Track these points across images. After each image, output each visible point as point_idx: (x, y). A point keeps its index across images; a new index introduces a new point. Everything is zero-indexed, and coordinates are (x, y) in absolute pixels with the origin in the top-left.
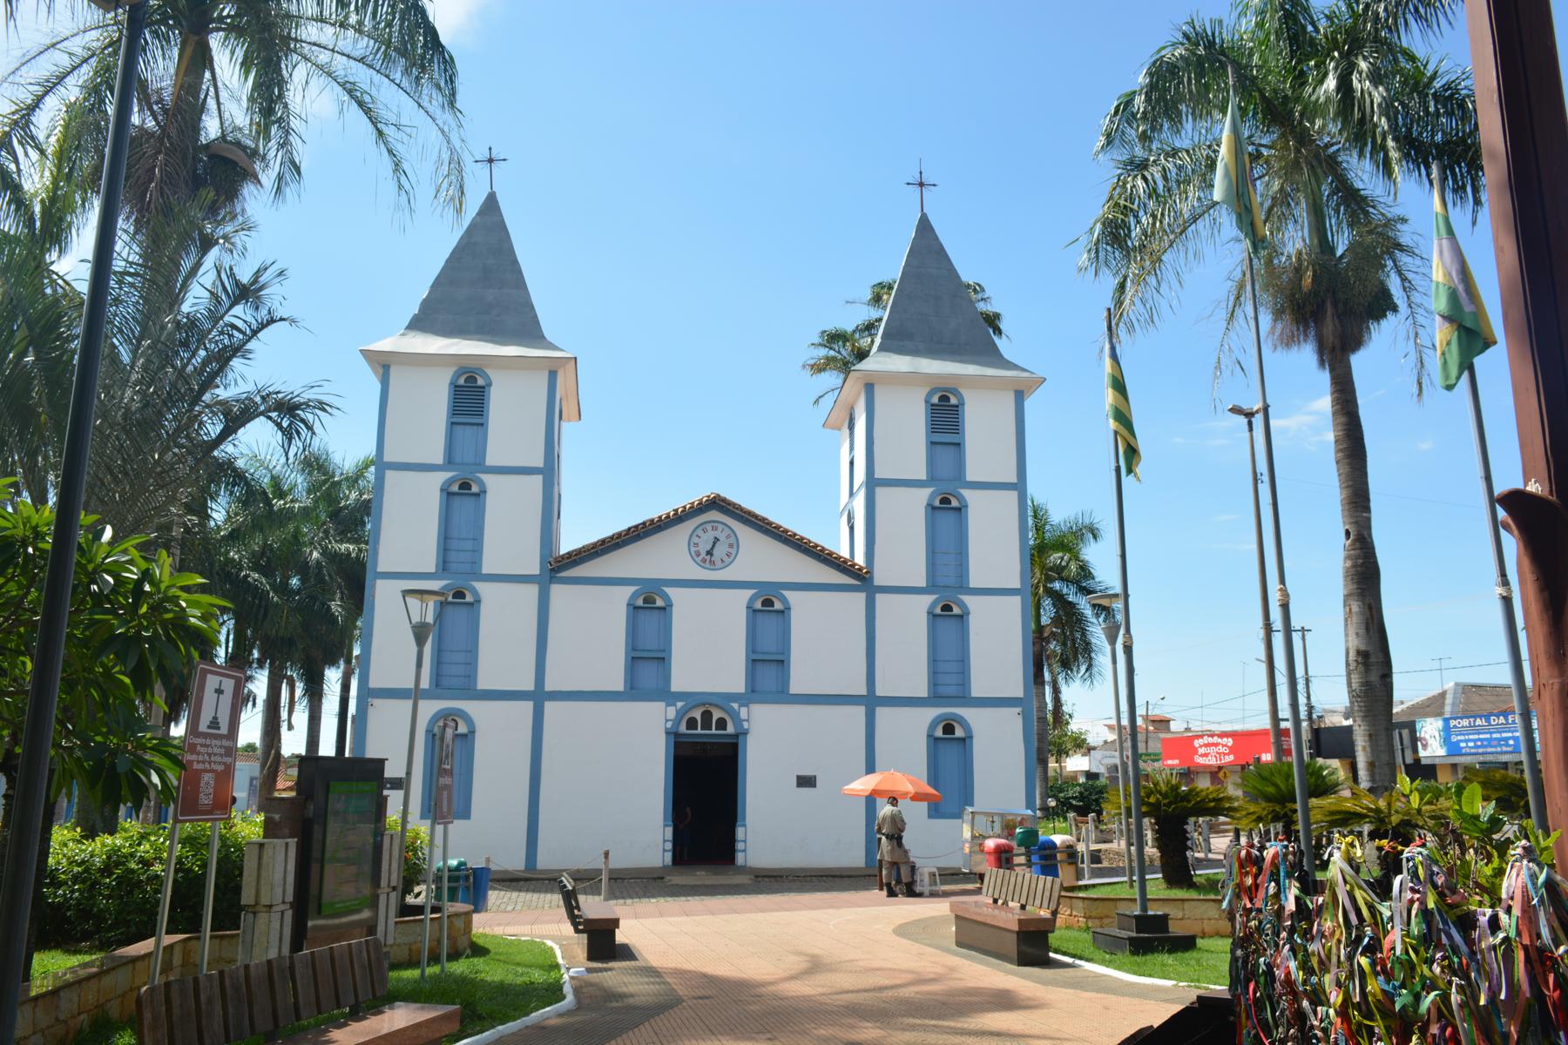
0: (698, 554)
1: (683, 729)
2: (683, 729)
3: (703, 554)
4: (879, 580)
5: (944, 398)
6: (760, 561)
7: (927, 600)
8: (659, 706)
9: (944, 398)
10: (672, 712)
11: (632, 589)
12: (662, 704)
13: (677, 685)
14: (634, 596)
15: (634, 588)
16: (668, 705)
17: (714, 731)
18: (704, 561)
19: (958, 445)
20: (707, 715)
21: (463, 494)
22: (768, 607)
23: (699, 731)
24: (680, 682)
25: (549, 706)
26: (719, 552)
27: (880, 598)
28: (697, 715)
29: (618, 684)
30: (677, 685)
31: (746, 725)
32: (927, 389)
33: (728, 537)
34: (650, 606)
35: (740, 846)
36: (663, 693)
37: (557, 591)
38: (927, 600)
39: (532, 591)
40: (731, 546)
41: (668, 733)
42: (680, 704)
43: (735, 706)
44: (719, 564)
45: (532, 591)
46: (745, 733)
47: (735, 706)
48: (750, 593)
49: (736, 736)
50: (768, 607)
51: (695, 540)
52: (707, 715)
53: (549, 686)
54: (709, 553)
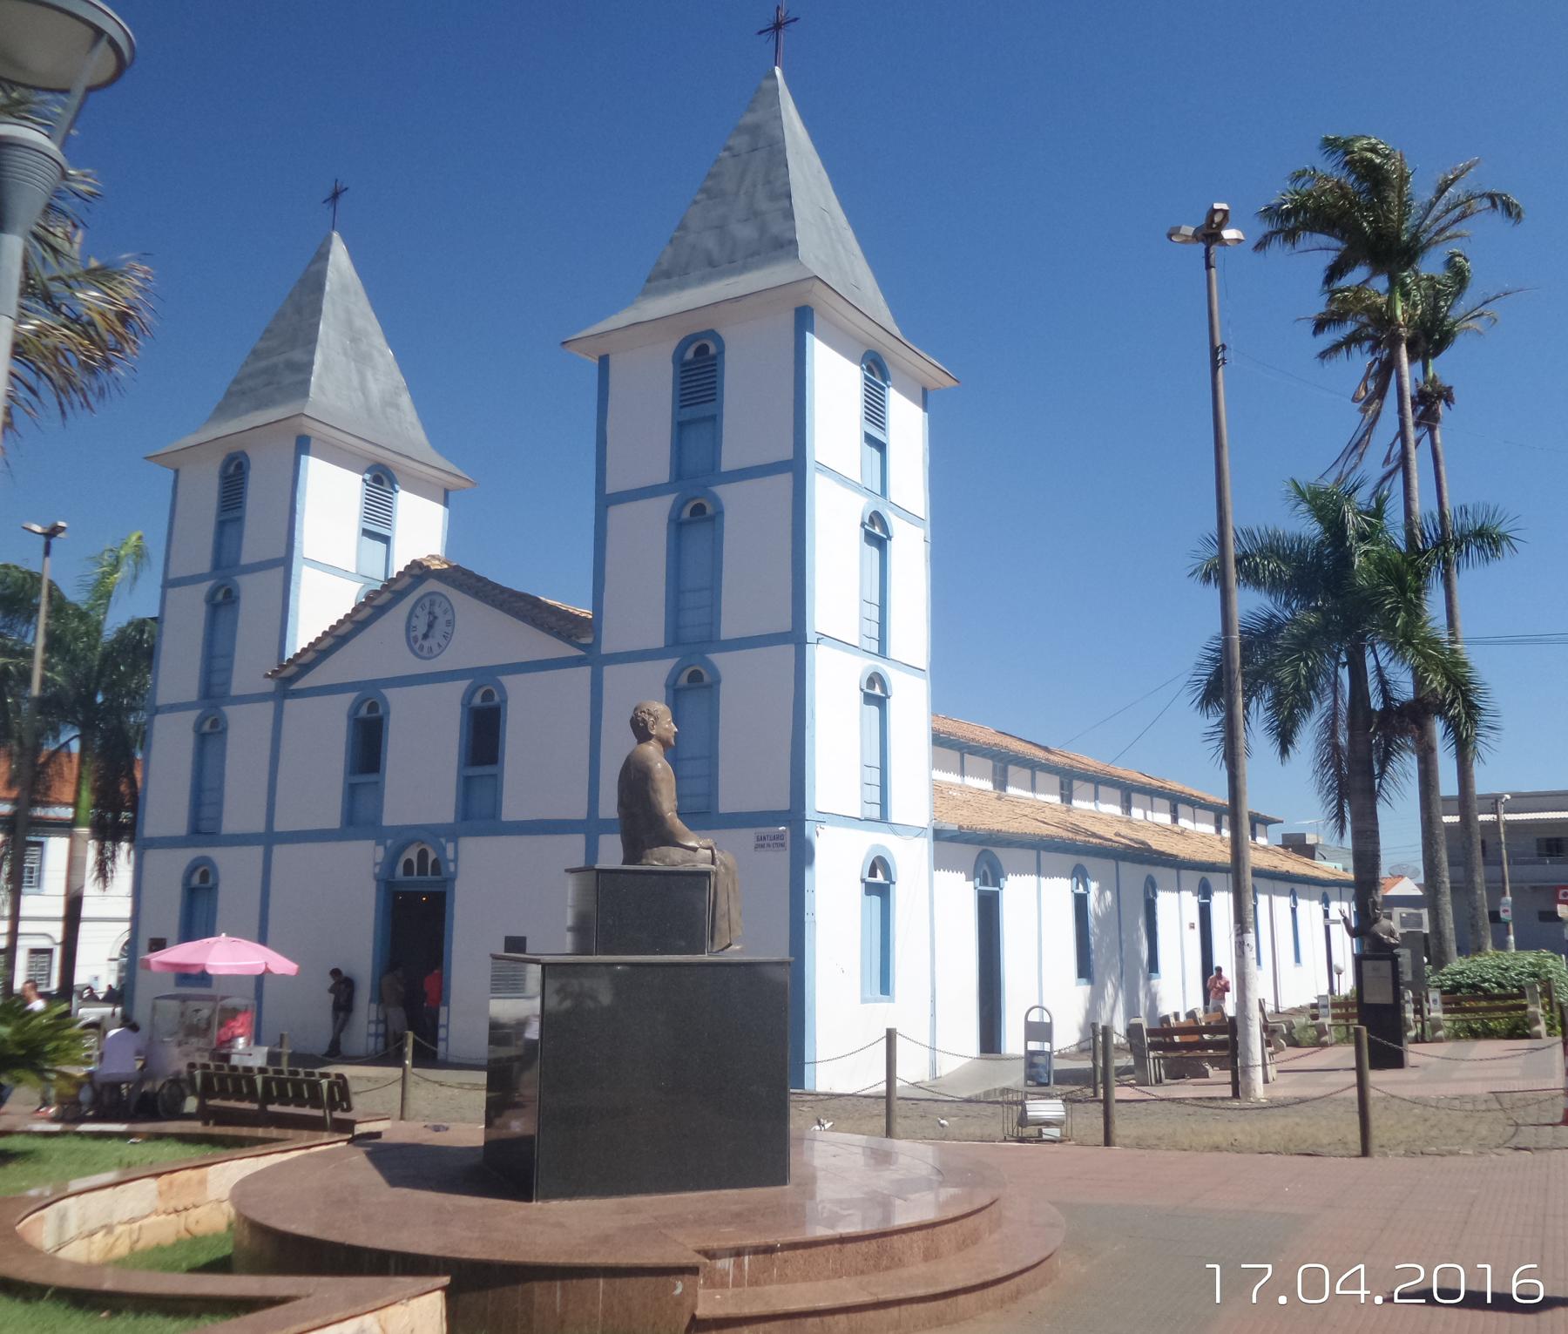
5: (702, 350)
7: (665, 666)
9: (702, 350)
10: (380, 853)
12: (371, 843)
13: (388, 820)
14: (355, 708)
16: (378, 844)
17: (430, 877)
19: (714, 420)
20: (423, 855)
25: (279, 851)
26: (440, 626)
27: (609, 671)
28: (412, 854)
29: (332, 818)
30: (388, 820)
31: (452, 867)
32: (675, 343)
33: (445, 612)
35: (442, 1033)
37: (290, 705)
38: (665, 666)
39: (268, 708)
41: (378, 879)
42: (389, 842)
43: (443, 840)
44: (436, 650)
45: (268, 708)
46: (452, 879)
47: (443, 840)
48: (462, 685)
49: (445, 881)
51: (415, 622)
52: (423, 855)
53: (280, 826)
54: (425, 636)
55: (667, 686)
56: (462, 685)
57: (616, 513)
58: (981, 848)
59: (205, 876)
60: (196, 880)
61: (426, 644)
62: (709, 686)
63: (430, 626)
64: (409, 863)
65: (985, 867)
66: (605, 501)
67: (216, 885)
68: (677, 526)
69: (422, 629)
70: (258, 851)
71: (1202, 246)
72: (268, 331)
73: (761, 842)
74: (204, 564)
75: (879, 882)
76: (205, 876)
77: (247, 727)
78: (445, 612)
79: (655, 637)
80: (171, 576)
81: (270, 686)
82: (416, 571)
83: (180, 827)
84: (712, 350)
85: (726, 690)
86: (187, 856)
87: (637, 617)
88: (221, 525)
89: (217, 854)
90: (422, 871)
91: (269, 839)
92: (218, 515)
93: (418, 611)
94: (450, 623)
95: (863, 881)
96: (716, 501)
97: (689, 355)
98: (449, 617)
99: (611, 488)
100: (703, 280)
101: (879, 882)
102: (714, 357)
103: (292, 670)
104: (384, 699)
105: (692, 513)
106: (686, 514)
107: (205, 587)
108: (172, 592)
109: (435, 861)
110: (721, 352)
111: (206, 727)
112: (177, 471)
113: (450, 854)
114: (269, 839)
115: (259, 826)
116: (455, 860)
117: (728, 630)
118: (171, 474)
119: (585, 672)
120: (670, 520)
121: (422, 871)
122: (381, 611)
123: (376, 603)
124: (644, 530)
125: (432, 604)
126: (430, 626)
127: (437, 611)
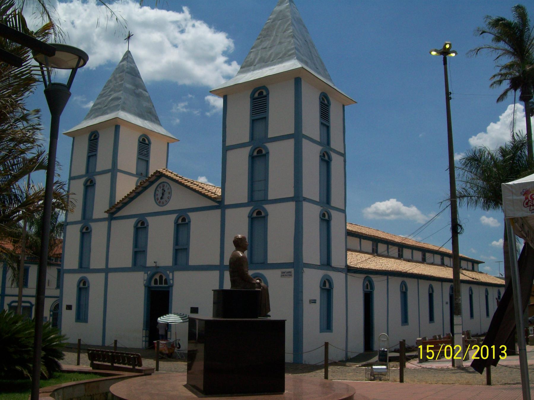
0: (158, 199)
1: (153, 284)
2: (153, 284)
3: (159, 199)
4: (227, 202)
5: (261, 93)
6: (178, 201)
8: (142, 274)
9: (261, 93)
11: (136, 219)
12: (142, 273)
15: (136, 219)
17: (163, 285)
18: (160, 202)
20: (161, 277)
21: (90, 185)
22: (182, 223)
23: (158, 285)
24: (150, 263)
25: (111, 275)
26: (166, 195)
28: (157, 277)
31: (171, 282)
32: (251, 91)
33: (168, 189)
34: (141, 227)
36: (144, 268)
37: (113, 222)
39: (106, 223)
40: (169, 193)
41: (145, 286)
42: (149, 272)
43: (168, 272)
44: (165, 203)
45: (106, 223)
46: (172, 286)
47: (168, 272)
49: (169, 287)
50: (182, 223)
51: (157, 192)
52: (161, 277)
53: (110, 266)
54: (162, 198)
55: (248, 217)
56: (174, 216)
57: (230, 154)
58: (366, 275)
59: (84, 284)
60: (81, 285)
61: (162, 201)
62: (264, 217)
63: (163, 194)
64: (156, 280)
65: (367, 282)
66: (226, 149)
67: (89, 286)
68: (252, 158)
69: (160, 196)
70: (103, 275)
71: (442, 56)
72: (105, 87)
73: (283, 275)
74: (83, 171)
75: (327, 288)
76: (84, 284)
77: (99, 231)
78: (168, 189)
79: (244, 199)
80: (72, 175)
81: (106, 215)
82: (158, 174)
83: (76, 266)
84: (265, 93)
85: (270, 219)
86: (77, 277)
87: (239, 192)
88: (89, 157)
89: (90, 277)
90: (161, 283)
91: (107, 271)
92: (88, 153)
93: (159, 189)
94: (170, 193)
95: (321, 288)
96: (266, 148)
97: (256, 95)
98: (169, 190)
99: (228, 144)
100: (261, 68)
101: (327, 288)
102: (266, 96)
103: (114, 210)
104: (147, 221)
105: (258, 153)
106: (255, 154)
107: (83, 180)
108: (71, 181)
109: (166, 280)
110: (268, 94)
111: (84, 230)
112: (74, 138)
113: (171, 277)
114: (107, 271)
115: (103, 266)
116: (173, 279)
117: (271, 197)
118: (72, 139)
119: (218, 212)
120: (250, 156)
121: (161, 283)
122: (146, 188)
123: (144, 186)
124: (240, 160)
125: (163, 186)
126: (163, 194)
127: (166, 189)
